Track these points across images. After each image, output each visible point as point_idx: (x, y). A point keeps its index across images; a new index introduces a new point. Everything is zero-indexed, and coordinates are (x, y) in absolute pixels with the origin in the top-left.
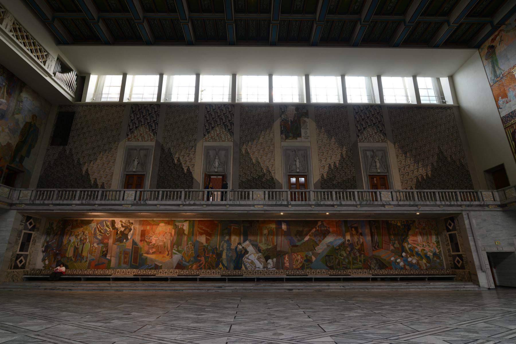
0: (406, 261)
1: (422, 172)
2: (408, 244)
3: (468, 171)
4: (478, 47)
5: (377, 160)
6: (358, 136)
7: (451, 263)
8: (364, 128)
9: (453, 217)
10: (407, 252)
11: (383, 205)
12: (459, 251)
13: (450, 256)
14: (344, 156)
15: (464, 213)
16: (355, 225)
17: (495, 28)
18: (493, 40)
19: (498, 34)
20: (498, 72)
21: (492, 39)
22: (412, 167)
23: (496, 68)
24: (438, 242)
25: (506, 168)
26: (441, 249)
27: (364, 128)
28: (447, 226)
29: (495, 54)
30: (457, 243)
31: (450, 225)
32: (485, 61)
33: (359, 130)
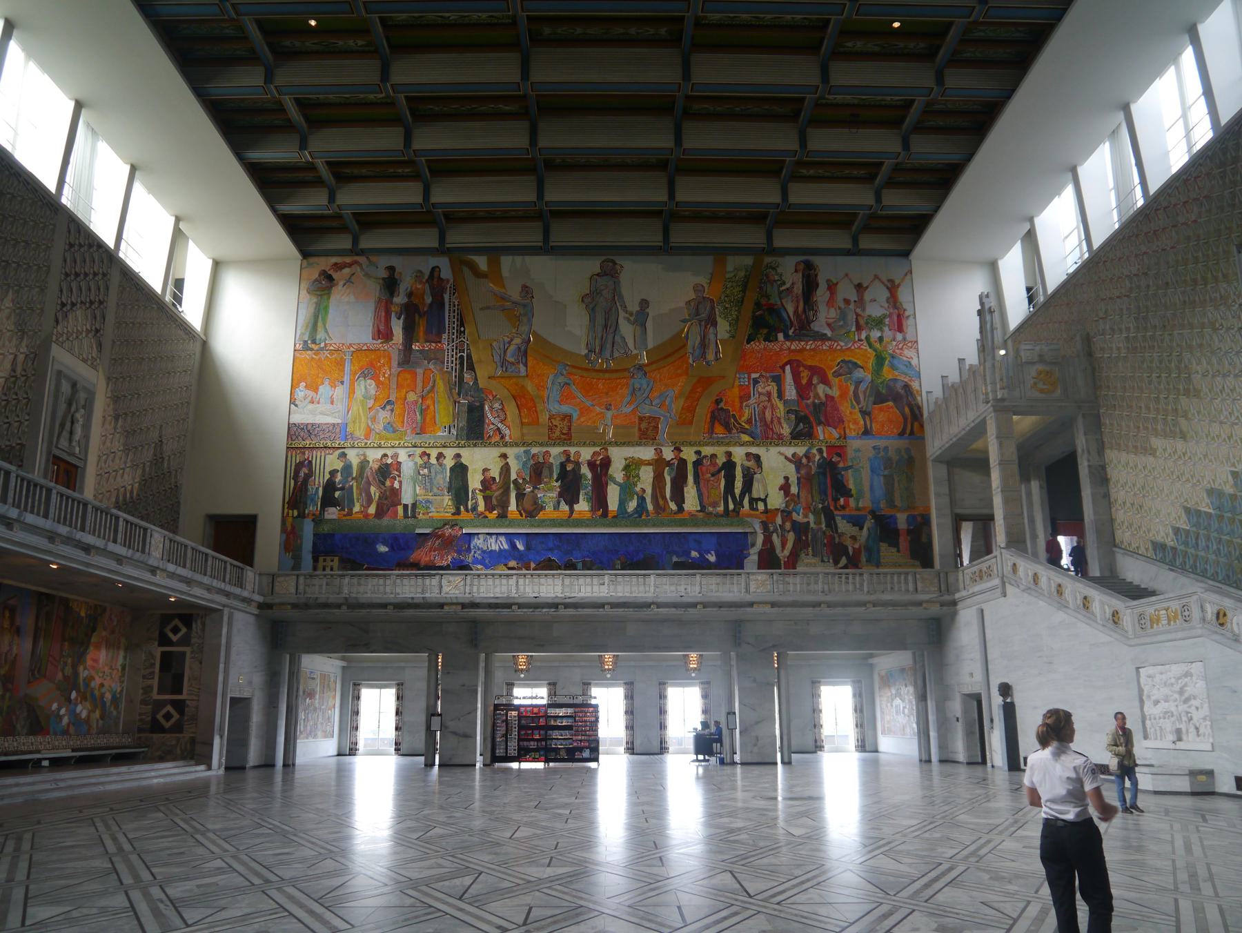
0: (73, 713)
1: (129, 480)
2: (85, 669)
3: (179, 503)
4: (305, 254)
5: (78, 416)
6: (57, 322)
7: (141, 720)
8: (73, 304)
9: (191, 615)
10: (78, 691)
11: (153, 570)
12: (181, 693)
13: (144, 702)
14: (19, 370)
15: (226, 611)
16: (12, 602)
17: (356, 251)
18: (338, 267)
19: (350, 265)
20: (321, 335)
21: (336, 264)
22: (117, 461)
23: (320, 324)
24: (124, 668)
25: (260, 525)
26: (125, 685)
27: (73, 304)
28: (173, 633)
29: (329, 294)
30: (182, 675)
31: (175, 630)
32: (304, 292)
33: (63, 305)
